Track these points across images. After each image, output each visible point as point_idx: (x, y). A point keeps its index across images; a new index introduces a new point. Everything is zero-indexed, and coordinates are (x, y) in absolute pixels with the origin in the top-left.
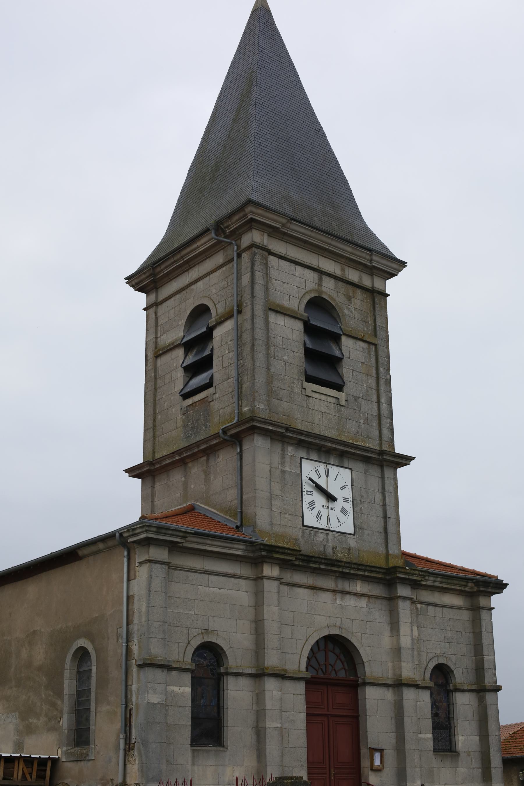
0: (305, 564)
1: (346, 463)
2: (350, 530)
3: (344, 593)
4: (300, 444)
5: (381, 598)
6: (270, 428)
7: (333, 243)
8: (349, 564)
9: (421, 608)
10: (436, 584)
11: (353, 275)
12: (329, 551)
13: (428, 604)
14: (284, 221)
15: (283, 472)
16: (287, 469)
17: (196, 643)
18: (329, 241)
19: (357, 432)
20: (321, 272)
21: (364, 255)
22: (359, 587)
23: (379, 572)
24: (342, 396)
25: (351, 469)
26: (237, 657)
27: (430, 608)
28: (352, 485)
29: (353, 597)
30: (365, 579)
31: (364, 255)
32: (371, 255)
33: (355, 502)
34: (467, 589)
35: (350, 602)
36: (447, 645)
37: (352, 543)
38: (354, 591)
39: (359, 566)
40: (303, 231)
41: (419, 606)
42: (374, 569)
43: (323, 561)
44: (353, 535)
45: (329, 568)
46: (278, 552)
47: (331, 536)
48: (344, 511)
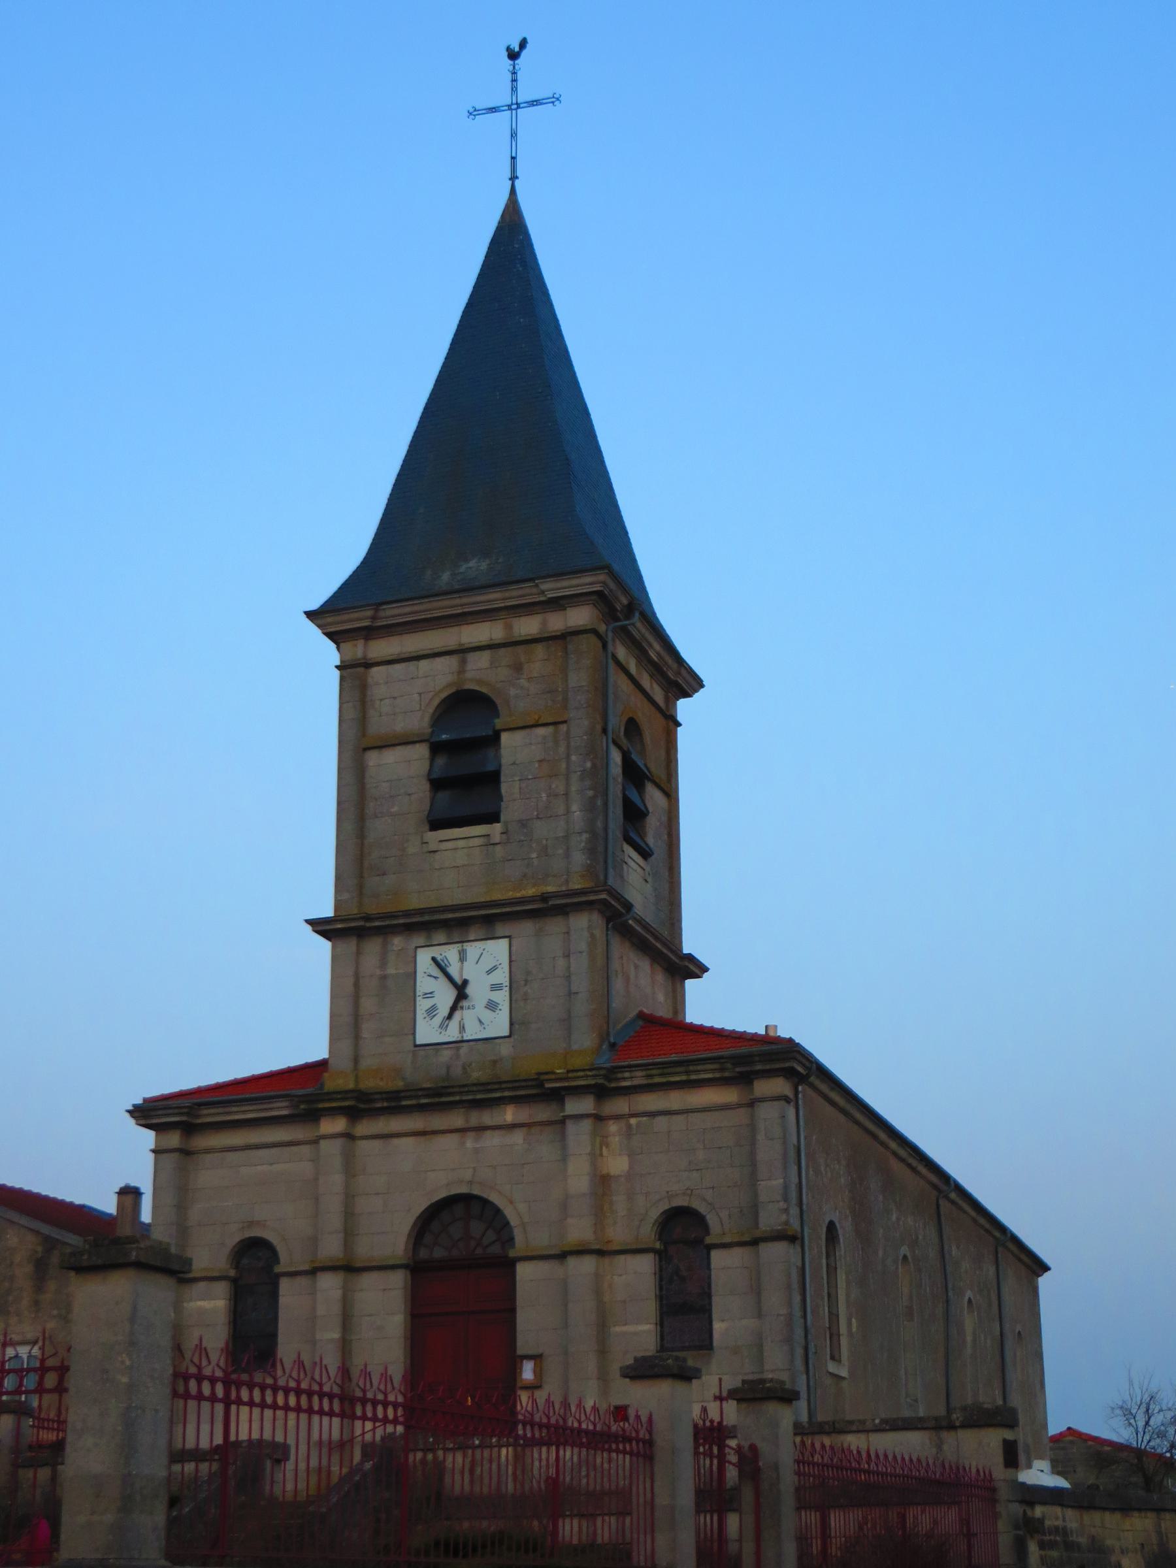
0: (393, 1104)
1: (500, 929)
2: (420, 1040)
3: (481, 1129)
4: (410, 929)
5: (739, 1105)
6: (339, 926)
7: (465, 600)
8: (484, 1086)
9: (638, 1125)
10: (657, 1080)
11: (528, 626)
12: (457, 1071)
13: (652, 1115)
14: (369, 613)
15: (384, 978)
16: (391, 971)
17: (234, 1239)
18: (458, 601)
19: (525, 876)
20: (462, 651)
21: (527, 591)
22: (509, 1114)
23: (527, 1087)
24: (497, 828)
25: (509, 937)
26: (719, 1224)
27: (661, 1121)
28: (511, 961)
29: (497, 1133)
30: (516, 1100)
31: (527, 591)
32: (537, 586)
33: (514, 986)
34: (727, 1074)
35: (492, 1140)
36: (695, 1174)
37: (505, 1050)
38: (501, 1123)
39: (499, 1084)
40: (408, 609)
41: (633, 1121)
42: (517, 1084)
43: (420, 1093)
44: (509, 1037)
45: (437, 1100)
46: (323, 1101)
47: (464, 1049)
48: (492, 1006)
